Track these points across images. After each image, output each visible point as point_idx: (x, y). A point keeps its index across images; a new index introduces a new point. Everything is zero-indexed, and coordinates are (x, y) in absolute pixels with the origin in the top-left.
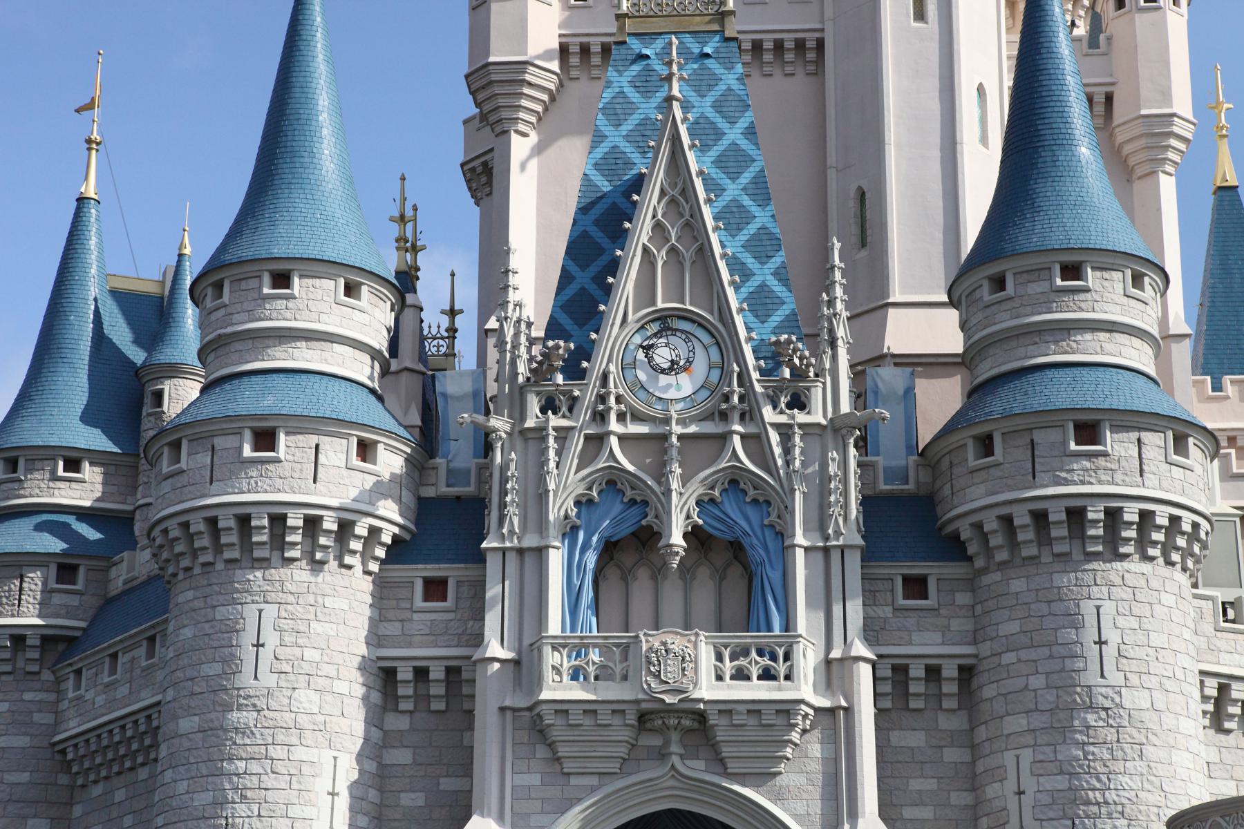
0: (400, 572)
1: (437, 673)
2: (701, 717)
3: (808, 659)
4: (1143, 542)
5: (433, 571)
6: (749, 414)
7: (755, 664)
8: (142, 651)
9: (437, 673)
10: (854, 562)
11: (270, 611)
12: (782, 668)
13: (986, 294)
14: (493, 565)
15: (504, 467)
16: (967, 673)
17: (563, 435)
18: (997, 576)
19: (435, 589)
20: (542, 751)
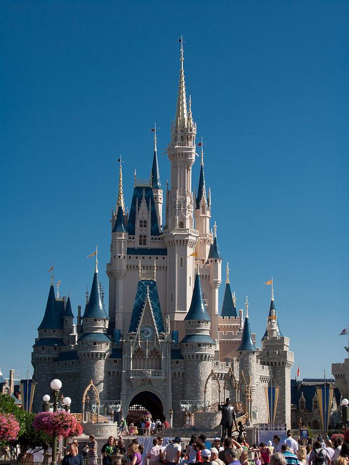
0: (111, 359)
1: (116, 372)
2: (150, 380)
3: (163, 374)
4: (205, 359)
5: (115, 359)
6: (157, 340)
7: (157, 374)
8: (71, 363)
9: (116, 372)
10: (170, 360)
11: (96, 366)
12: (160, 374)
13: (188, 323)
14: (124, 359)
15: (125, 346)
16: (183, 373)
17: (133, 343)
18: (187, 362)
19: (115, 361)
20: (130, 384)
